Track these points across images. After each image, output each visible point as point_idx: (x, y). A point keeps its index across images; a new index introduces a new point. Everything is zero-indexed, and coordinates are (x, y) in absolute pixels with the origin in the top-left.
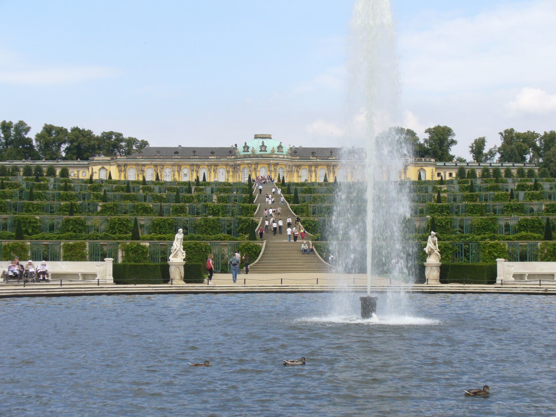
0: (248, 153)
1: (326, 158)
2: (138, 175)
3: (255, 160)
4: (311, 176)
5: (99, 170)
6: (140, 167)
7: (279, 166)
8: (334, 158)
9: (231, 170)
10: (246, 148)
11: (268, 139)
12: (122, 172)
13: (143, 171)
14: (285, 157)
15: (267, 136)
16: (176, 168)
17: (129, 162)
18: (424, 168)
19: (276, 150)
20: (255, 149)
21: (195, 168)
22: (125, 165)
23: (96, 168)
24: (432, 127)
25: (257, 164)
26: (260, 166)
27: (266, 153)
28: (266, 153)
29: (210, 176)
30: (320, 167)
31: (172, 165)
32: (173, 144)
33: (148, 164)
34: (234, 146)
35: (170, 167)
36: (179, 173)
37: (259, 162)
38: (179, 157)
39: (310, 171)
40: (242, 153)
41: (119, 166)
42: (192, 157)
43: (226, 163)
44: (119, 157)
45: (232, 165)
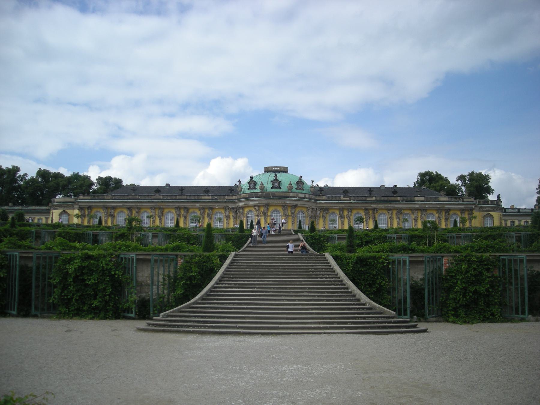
0: (255, 191)
1: (362, 198)
3: (264, 201)
4: (343, 224)
5: (60, 215)
6: (109, 210)
7: (298, 209)
8: (374, 198)
9: (231, 215)
10: (252, 183)
11: (284, 174)
13: (113, 216)
14: (307, 196)
15: (282, 169)
17: (94, 204)
18: (491, 213)
19: (295, 187)
20: (265, 185)
21: (183, 212)
24: (466, 173)
25: (267, 206)
26: (271, 209)
27: (280, 190)
28: (280, 190)
30: (354, 212)
31: (151, 208)
32: (158, 182)
33: (120, 207)
34: (238, 184)
36: (161, 219)
37: (270, 202)
38: (161, 197)
39: (342, 217)
40: (247, 191)
42: (178, 197)
43: (225, 205)
44: (81, 197)
45: (233, 208)
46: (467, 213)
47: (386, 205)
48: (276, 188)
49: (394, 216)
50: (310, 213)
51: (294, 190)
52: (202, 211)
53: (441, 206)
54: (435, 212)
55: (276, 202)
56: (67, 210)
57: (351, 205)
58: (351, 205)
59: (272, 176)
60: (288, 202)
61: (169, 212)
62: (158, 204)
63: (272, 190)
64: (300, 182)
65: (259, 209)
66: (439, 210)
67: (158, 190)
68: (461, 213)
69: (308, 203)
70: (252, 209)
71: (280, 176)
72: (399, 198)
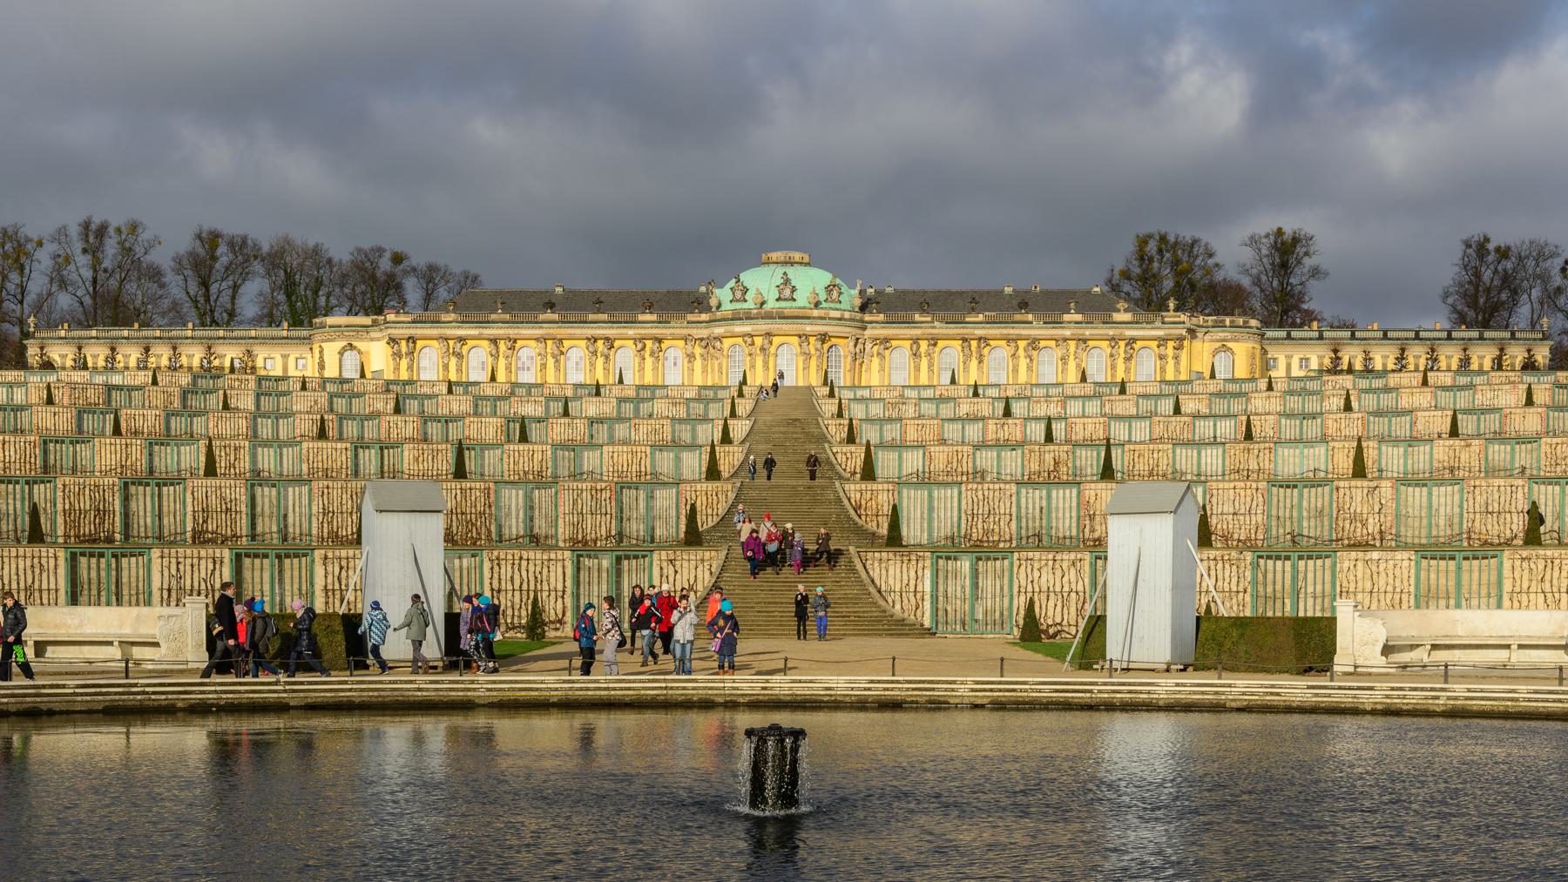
0: (745, 306)
2: (446, 367)
3: (763, 326)
4: (917, 369)
5: (341, 353)
6: (451, 343)
8: (981, 317)
9: (698, 351)
13: (459, 356)
17: (419, 332)
18: (1229, 345)
19: (823, 296)
23: (332, 349)
29: (642, 369)
31: (537, 340)
35: (533, 343)
36: (557, 361)
41: (393, 341)
42: (591, 317)
46: (1171, 344)
47: (1005, 331)
52: (640, 346)
55: (785, 327)
60: (808, 328)
66: (1113, 340)
72: (1030, 317)
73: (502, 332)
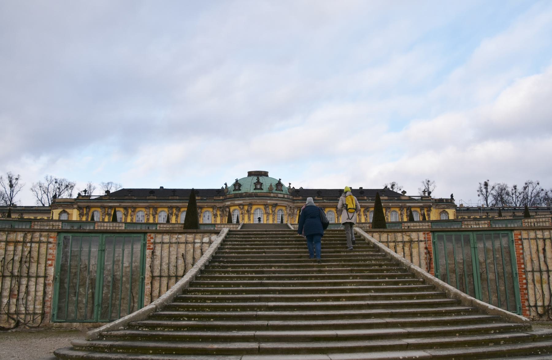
0: (240, 192)
2: (103, 219)
3: (248, 201)
6: (107, 209)
7: (278, 208)
9: (219, 213)
10: (237, 185)
12: (83, 216)
14: (286, 196)
16: (151, 211)
17: (92, 204)
18: (446, 210)
21: (174, 210)
22: (88, 207)
25: (251, 205)
26: (254, 207)
27: (262, 191)
28: (262, 191)
32: (155, 185)
35: (144, 209)
36: (154, 218)
38: (155, 198)
40: (233, 192)
41: (79, 208)
42: (170, 198)
43: (213, 204)
45: (220, 208)
46: (425, 210)
48: (258, 189)
49: (362, 213)
50: (288, 211)
51: (274, 191)
53: (403, 204)
54: (397, 210)
55: (258, 201)
56: (67, 210)
57: (324, 204)
58: (324, 204)
59: (255, 179)
60: (269, 202)
61: (162, 211)
62: (152, 204)
63: (255, 191)
64: (279, 184)
65: (243, 208)
66: (401, 208)
67: (152, 192)
68: (421, 210)
69: (287, 203)
70: (237, 207)
71: (262, 179)
72: (365, 198)
73: (129, 204)
